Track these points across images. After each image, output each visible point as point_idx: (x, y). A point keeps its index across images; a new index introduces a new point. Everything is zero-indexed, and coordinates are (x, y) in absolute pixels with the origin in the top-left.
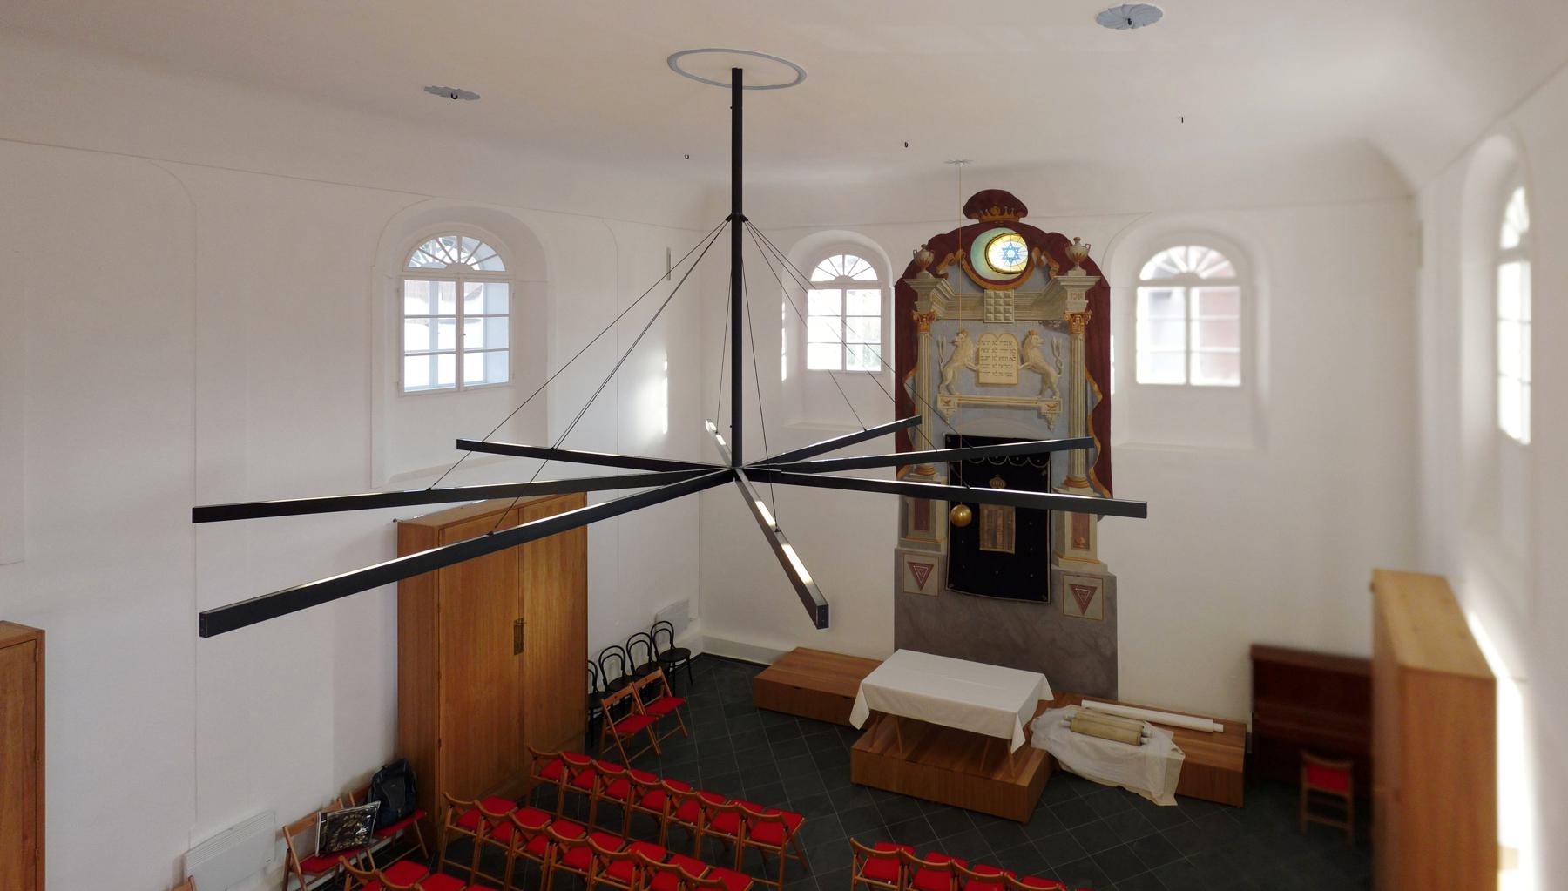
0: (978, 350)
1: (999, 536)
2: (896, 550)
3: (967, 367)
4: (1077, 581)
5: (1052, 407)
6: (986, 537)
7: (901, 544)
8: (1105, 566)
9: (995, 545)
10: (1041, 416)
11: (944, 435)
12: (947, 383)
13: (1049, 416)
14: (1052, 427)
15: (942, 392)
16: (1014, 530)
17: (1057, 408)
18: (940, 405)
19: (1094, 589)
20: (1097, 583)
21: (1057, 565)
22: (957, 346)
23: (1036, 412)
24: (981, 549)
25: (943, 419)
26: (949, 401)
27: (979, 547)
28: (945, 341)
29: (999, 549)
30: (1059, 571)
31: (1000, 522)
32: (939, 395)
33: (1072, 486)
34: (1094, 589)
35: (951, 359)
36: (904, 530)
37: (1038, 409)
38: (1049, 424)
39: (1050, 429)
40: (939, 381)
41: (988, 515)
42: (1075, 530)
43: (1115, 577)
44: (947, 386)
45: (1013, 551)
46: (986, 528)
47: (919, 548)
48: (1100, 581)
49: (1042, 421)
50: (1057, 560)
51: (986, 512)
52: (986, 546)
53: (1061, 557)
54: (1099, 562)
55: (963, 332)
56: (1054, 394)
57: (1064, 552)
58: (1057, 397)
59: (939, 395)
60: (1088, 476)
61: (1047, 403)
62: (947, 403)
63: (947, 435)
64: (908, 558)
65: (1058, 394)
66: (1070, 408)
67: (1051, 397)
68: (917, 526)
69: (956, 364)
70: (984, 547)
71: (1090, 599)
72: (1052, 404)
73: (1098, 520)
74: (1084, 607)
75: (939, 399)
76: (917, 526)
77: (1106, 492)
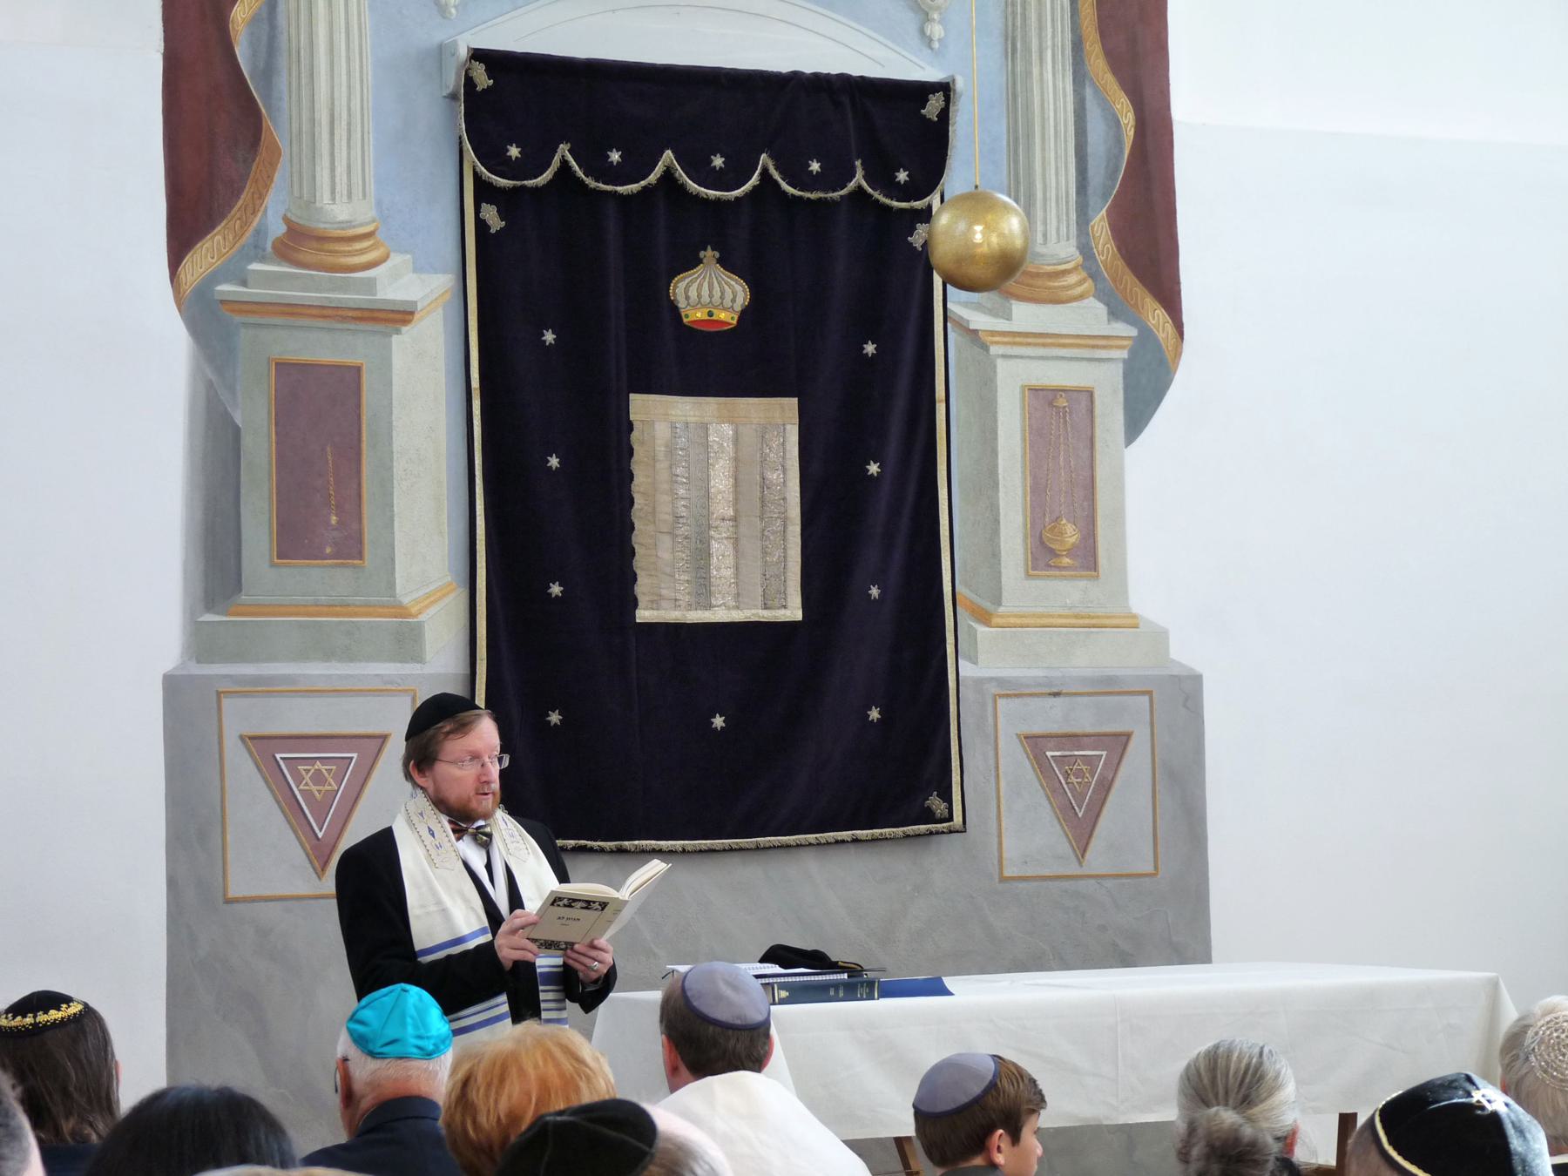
1: (721, 550)
4: (1050, 717)
6: (666, 555)
7: (201, 643)
8: (1160, 637)
9: (703, 591)
16: (795, 512)
19: (1119, 742)
20: (1131, 717)
21: (974, 660)
24: (644, 615)
27: (635, 603)
29: (721, 614)
30: (979, 682)
31: (721, 481)
34: (1119, 742)
41: (671, 451)
42: (1038, 490)
43: (1197, 680)
45: (792, 611)
46: (664, 514)
47: (302, 656)
48: (1146, 698)
50: (973, 634)
51: (662, 431)
53: (985, 618)
54: (1132, 622)
60: (1085, 250)
64: (241, 718)
70: (655, 604)
71: (1105, 787)
73: (1126, 447)
74: (1081, 831)
77: (1157, 316)
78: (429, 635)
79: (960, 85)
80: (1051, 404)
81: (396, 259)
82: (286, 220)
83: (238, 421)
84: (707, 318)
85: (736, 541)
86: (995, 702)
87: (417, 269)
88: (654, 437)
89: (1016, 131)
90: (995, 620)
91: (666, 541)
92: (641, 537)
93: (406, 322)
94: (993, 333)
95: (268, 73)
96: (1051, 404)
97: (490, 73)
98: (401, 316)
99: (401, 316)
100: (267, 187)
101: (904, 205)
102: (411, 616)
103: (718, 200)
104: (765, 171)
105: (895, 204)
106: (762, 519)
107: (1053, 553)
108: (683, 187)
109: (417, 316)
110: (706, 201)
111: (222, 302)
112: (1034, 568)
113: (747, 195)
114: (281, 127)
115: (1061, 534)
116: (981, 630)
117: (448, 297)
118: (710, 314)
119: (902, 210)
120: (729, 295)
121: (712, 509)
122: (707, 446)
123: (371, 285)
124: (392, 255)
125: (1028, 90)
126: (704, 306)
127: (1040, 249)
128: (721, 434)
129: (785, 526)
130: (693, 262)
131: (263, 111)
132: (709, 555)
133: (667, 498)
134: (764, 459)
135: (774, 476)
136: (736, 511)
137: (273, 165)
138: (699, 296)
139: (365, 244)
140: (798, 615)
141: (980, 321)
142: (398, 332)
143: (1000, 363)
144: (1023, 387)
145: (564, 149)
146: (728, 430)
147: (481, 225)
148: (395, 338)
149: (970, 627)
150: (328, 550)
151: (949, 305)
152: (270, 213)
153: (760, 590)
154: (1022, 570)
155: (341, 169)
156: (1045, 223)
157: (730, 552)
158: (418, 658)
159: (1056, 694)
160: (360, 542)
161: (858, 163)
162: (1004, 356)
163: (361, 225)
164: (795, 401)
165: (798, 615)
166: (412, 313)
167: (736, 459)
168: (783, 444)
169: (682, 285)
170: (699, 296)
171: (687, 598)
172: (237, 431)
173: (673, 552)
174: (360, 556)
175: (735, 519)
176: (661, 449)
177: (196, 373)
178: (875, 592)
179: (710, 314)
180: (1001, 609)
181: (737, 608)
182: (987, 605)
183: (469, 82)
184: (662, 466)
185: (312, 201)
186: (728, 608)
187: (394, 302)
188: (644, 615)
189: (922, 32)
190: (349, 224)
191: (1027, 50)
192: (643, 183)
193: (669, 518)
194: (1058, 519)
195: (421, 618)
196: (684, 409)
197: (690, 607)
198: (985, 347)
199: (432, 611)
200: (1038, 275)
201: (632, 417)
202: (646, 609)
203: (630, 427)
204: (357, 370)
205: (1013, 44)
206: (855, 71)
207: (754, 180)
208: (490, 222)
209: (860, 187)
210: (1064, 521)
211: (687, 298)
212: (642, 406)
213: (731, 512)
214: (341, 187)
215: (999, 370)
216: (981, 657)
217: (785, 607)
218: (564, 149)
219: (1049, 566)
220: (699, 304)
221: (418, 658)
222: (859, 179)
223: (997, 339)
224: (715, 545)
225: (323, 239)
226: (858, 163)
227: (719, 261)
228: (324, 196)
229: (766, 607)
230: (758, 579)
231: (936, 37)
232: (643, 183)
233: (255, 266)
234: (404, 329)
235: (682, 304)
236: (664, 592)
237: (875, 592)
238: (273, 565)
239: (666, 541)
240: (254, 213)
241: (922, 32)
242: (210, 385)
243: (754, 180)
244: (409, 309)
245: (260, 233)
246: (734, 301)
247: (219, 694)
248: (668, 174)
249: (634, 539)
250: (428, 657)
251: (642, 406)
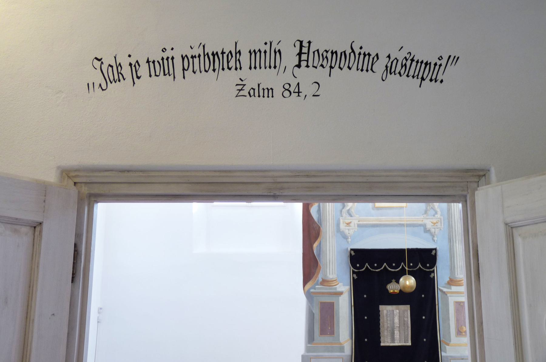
1: (397, 332)
2: (303, 357)
5: (434, 224)
6: (386, 334)
7: (308, 350)
9: (393, 340)
10: (427, 231)
11: (349, 249)
13: (433, 230)
14: (435, 239)
15: (344, 215)
17: (439, 223)
18: (342, 226)
21: (446, 352)
23: (422, 228)
24: (382, 344)
25: (345, 237)
26: (350, 222)
27: (380, 342)
29: (397, 344)
30: (447, 357)
31: (396, 320)
32: (341, 218)
33: (453, 285)
36: (310, 337)
37: (424, 226)
38: (434, 237)
39: (434, 241)
41: (387, 315)
44: (348, 210)
45: (409, 344)
46: (386, 326)
49: (427, 235)
50: (445, 348)
51: (385, 312)
52: (386, 341)
53: (448, 345)
56: (436, 213)
57: (450, 341)
58: (438, 216)
59: (341, 218)
61: (431, 220)
62: (348, 224)
63: (352, 250)
65: (439, 213)
66: (449, 222)
67: (434, 216)
68: (323, 332)
70: (384, 342)
72: (435, 221)
75: (341, 221)
76: (323, 332)
78: (345, 348)
79: (438, 249)
80: (460, 305)
81: (340, 284)
82: (322, 278)
83: (314, 312)
84: (393, 291)
85: (399, 331)
86: (450, 361)
87: (344, 285)
88: (383, 313)
89: (451, 255)
90: (450, 345)
91: (386, 331)
92: (382, 329)
93: (342, 294)
94: (448, 292)
95: (319, 255)
96: (460, 305)
97: (354, 252)
98: (341, 293)
99: (341, 293)
100: (319, 273)
101: (429, 270)
102: (342, 345)
103: (394, 271)
104: (403, 266)
105: (427, 270)
106: (404, 327)
107: (461, 332)
108: (388, 269)
109: (343, 293)
110: (392, 272)
111: (312, 293)
112: (457, 335)
113: (399, 270)
114: (321, 264)
115: (462, 329)
116: (447, 347)
117: (349, 290)
118: (394, 291)
119: (428, 271)
120: (397, 287)
121: (395, 325)
122: (393, 314)
123: (336, 288)
124: (339, 283)
125: (453, 248)
126: (393, 289)
127: (456, 276)
128: (397, 312)
129: (408, 328)
130: (390, 282)
131: (318, 261)
132: (394, 333)
133: (386, 324)
134: (404, 316)
135: (406, 319)
136: (399, 326)
137: (320, 270)
138: (392, 288)
139: (335, 282)
140: (410, 344)
141: (445, 290)
142: (340, 296)
143: (449, 298)
144: (454, 302)
145: (367, 264)
146: (398, 311)
147: (353, 278)
148: (340, 297)
149: (445, 346)
150: (328, 333)
151: (438, 287)
152: (319, 278)
153: (404, 340)
154: (455, 335)
155: (331, 270)
156: (457, 271)
157: (398, 333)
158: (344, 352)
159: (463, 359)
160: (334, 332)
161: (420, 263)
162: (450, 296)
163: (334, 279)
164: (409, 306)
165: (410, 344)
166: (343, 293)
167: (399, 316)
168: (407, 313)
169: (389, 286)
170: (392, 288)
171: (390, 341)
172: (314, 314)
173: (387, 333)
174: (334, 334)
175: (399, 327)
176: (385, 315)
177: (307, 304)
178: (425, 340)
179: (394, 291)
180: (451, 343)
181: (400, 343)
182: (448, 342)
183: (351, 254)
184: (385, 318)
185: (326, 275)
186: (398, 343)
187: (339, 291)
188: (382, 344)
189: (433, 239)
190: (332, 278)
191: (453, 241)
192: (381, 269)
193: (386, 327)
194: (462, 326)
195: (344, 345)
196: (389, 308)
197: (390, 343)
198: (446, 295)
199: (346, 344)
200: (457, 281)
201: (380, 309)
202: (382, 343)
203: (379, 311)
204: (333, 303)
205: (450, 240)
206: (419, 247)
207: (401, 267)
208: (355, 277)
209: (420, 267)
210: (463, 326)
211: (390, 288)
212: (381, 307)
213: (398, 326)
214: (331, 272)
215: (449, 299)
216: (447, 352)
217: (408, 343)
218: (367, 264)
219: (460, 335)
220: (392, 289)
221: (344, 352)
222: (420, 265)
223: (449, 293)
224: (396, 332)
225: (328, 281)
226: (420, 263)
227: (395, 282)
228: (328, 275)
229: (405, 343)
230: (403, 338)
231: (435, 240)
232: (381, 269)
233: (317, 286)
234: (342, 296)
235: (389, 289)
236: (386, 340)
237: (425, 340)
238: (319, 336)
239: (386, 331)
240: (317, 278)
241: (433, 239)
242: (309, 306)
243: (401, 267)
244: (342, 292)
245: (318, 281)
246: (398, 288)
247: (310, 358)
248: (385, 267)
249: (380, 331)
250: (345, 352)
251: (381, 307)
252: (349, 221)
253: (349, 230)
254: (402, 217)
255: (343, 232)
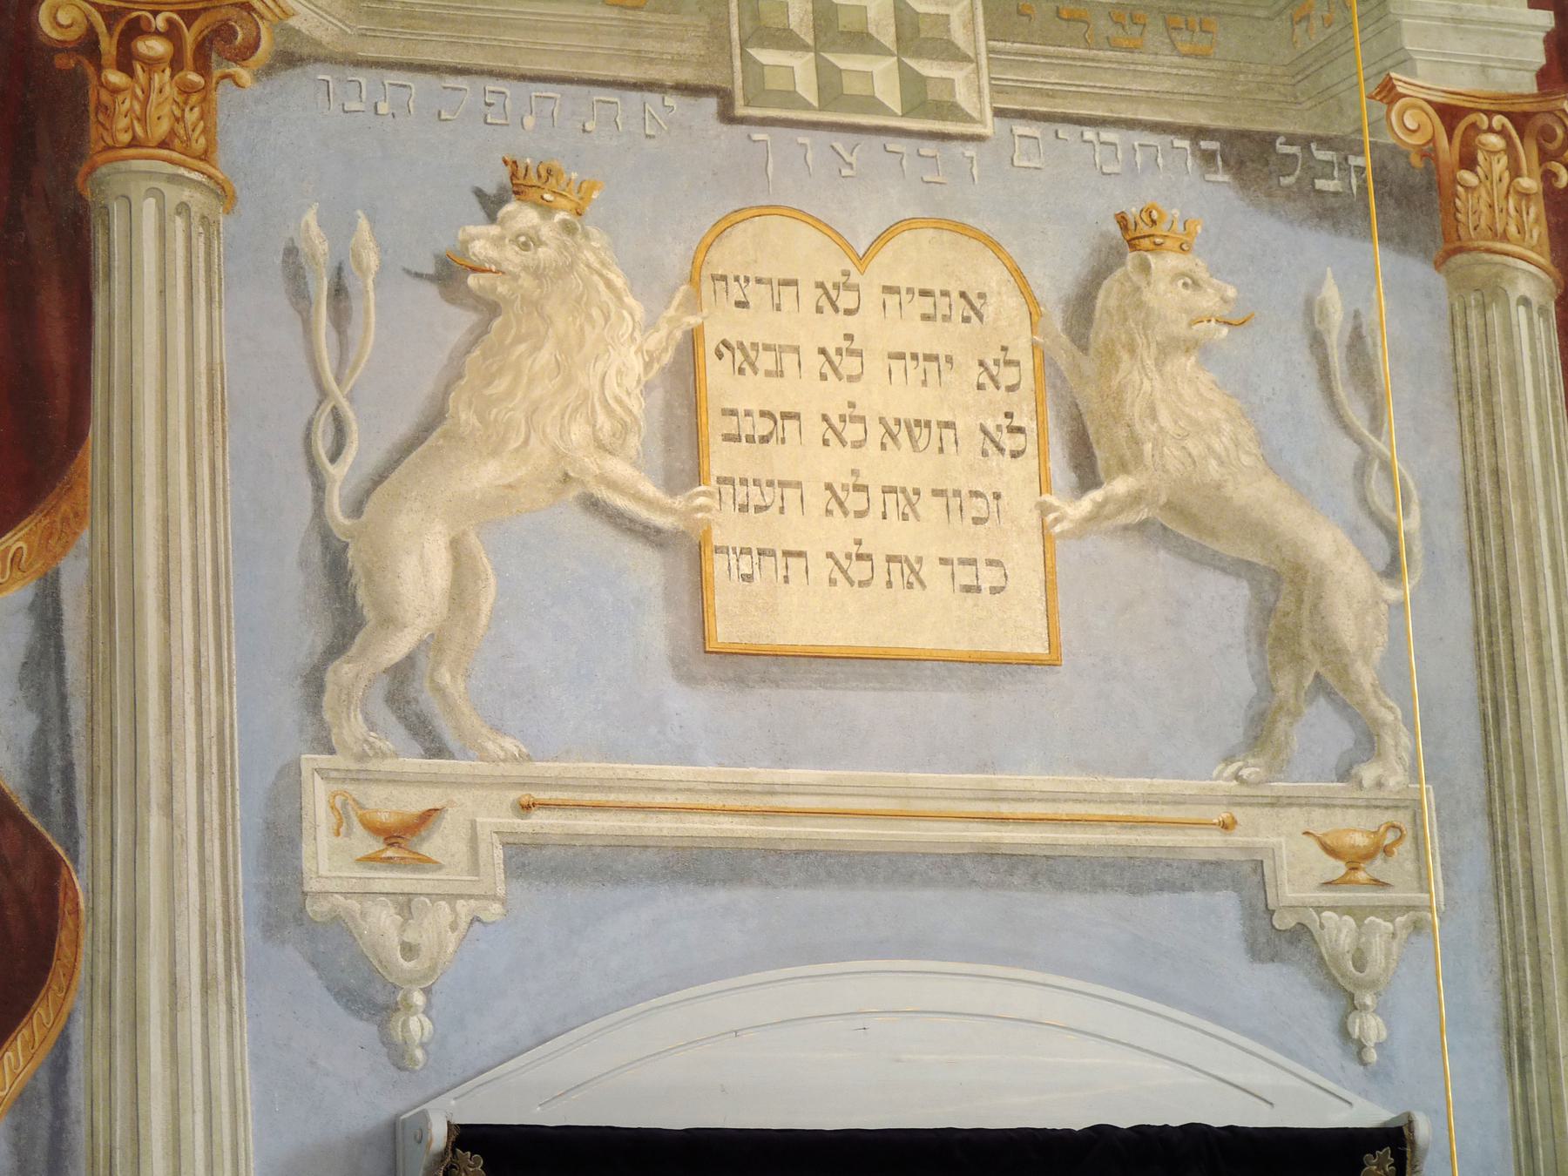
0: (693, 339)
3: (593, 505)
5: (1356, 859)
12: (398, 647)
13: (1339, 933)
14: (1371, 1027)
15: (352, 729)
22: (490, 308)
23: (1226, 903)
26: (428, 817)
28: (372, 259)
35: (433, 421)
38: (1352, 1005)
40: (314, 638)
44: (402, 673)
55: (519, 184)
61: (1321, 821)
69: (486, 475)
75: (318, 799)
252: (414, 802)
253: (406, 904)
254: (1006, 780)
255: (339, 925)
